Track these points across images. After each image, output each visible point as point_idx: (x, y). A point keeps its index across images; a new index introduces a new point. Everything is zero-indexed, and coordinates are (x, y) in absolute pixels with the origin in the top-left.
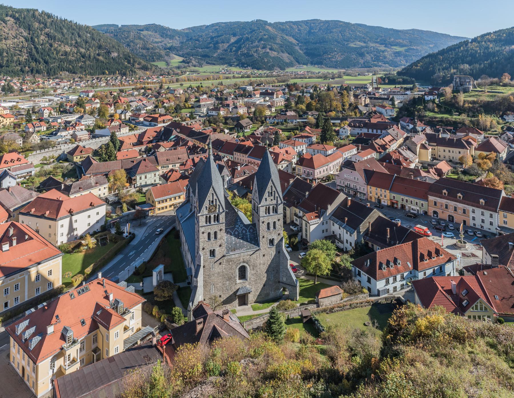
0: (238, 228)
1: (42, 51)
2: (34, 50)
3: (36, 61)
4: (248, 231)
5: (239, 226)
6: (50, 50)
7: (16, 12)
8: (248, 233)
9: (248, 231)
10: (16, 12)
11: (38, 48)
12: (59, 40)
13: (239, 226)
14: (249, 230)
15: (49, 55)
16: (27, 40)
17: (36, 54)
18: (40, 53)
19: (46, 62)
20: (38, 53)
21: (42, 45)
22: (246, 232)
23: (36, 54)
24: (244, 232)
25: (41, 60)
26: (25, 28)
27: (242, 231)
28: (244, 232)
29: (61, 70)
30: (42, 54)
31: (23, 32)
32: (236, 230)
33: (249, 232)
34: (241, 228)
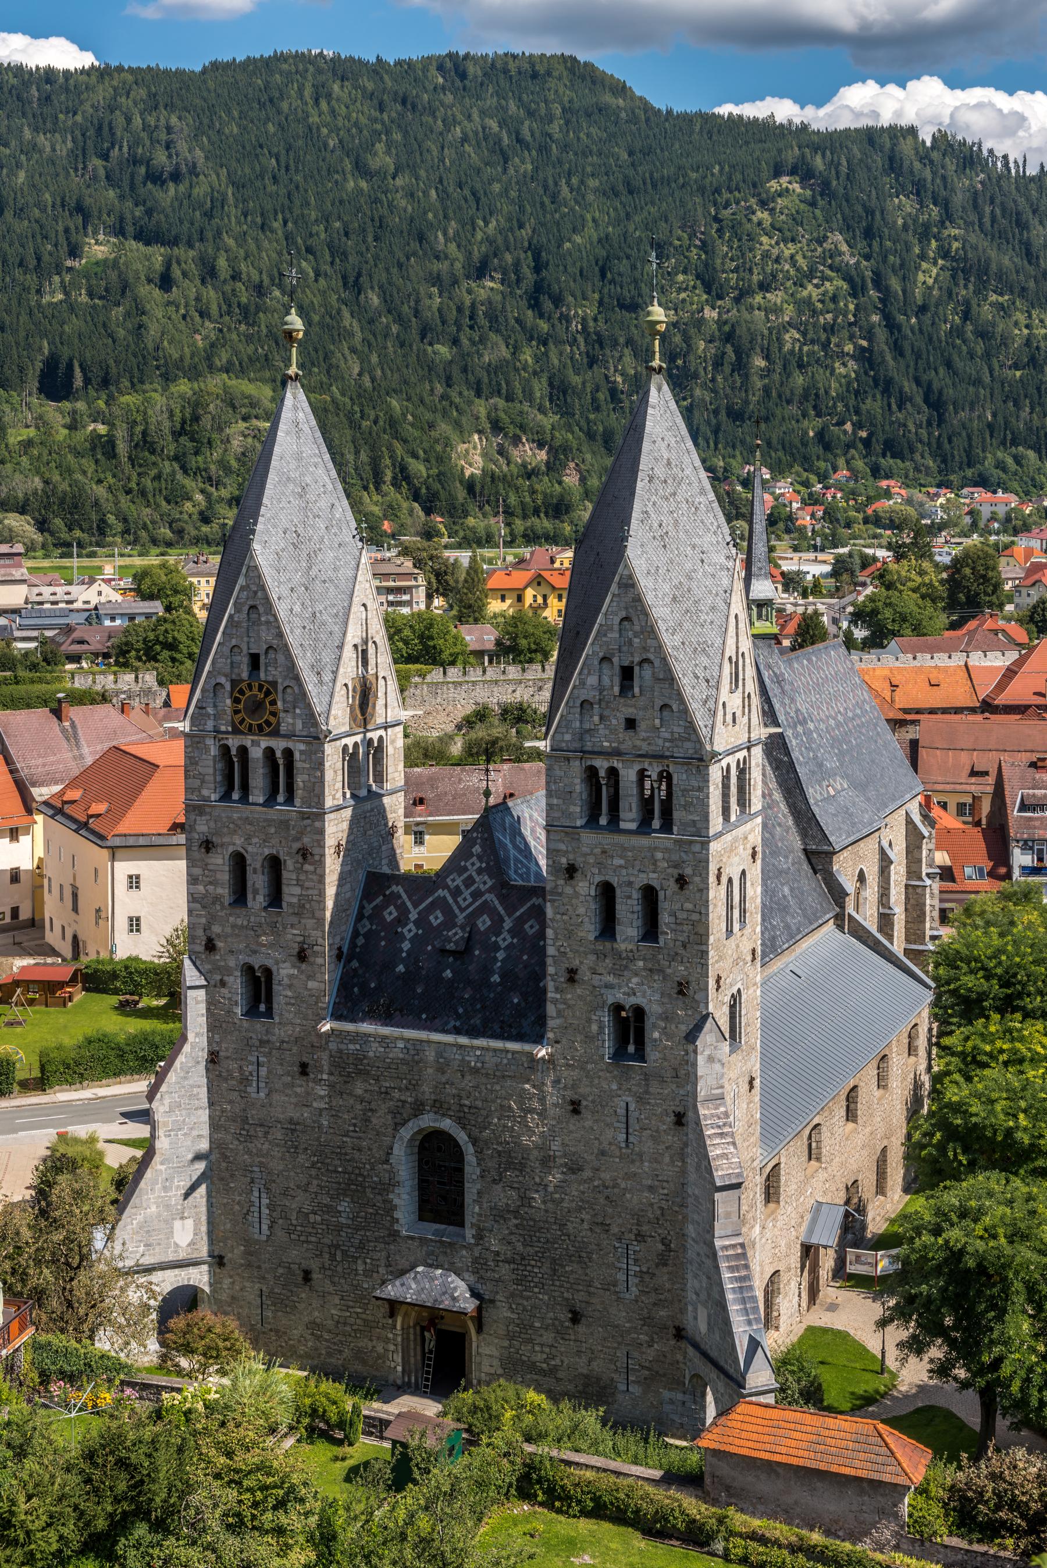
0: (456, 893)
1: (921, 344)
2: (881, 335)
3: (886, 386)
4: (508, 924)
5: (469, 882)
6: (957, 332)
7: (816, 148)
8: (504, 939)
9: (508, 924)
10: (816, 148)
11: (899, 328)
12: (1005, 285)
13: (469, 882)
14: (520, 921)
15: (949, 365)
16: (856, 289)
17: (889, 357)
18: (908, 352)
19: (935, 403)
20: (898, 350)
21: (923, 309)
22: (496, 927)
23: (889, 357)
24: (484, 923)
25: (908, 387)
26: (847, 228)
27: (472, 918)
28: (484, 923)
29: (1003, 443)
30: (918, 356)
31: (844, 248)
32: (440, 904)
33: (517, 931)
34: (476, 895)
